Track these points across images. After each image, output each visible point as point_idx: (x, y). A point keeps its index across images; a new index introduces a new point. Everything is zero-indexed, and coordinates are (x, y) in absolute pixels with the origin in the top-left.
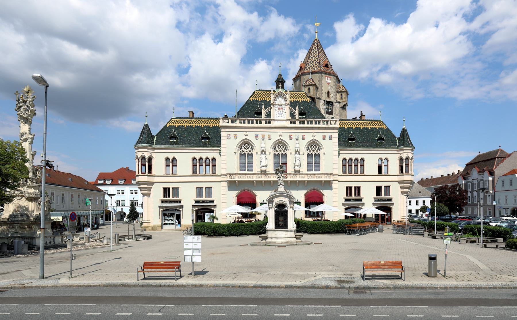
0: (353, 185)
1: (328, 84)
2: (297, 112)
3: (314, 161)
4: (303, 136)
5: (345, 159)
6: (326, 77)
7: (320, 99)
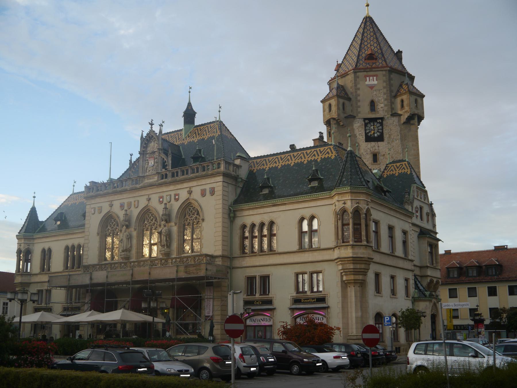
1: (372, 87)
2: (169, 161)
4: (175, 195)
5: (244, 226)
6: (366, 77)
7: (354, 117)
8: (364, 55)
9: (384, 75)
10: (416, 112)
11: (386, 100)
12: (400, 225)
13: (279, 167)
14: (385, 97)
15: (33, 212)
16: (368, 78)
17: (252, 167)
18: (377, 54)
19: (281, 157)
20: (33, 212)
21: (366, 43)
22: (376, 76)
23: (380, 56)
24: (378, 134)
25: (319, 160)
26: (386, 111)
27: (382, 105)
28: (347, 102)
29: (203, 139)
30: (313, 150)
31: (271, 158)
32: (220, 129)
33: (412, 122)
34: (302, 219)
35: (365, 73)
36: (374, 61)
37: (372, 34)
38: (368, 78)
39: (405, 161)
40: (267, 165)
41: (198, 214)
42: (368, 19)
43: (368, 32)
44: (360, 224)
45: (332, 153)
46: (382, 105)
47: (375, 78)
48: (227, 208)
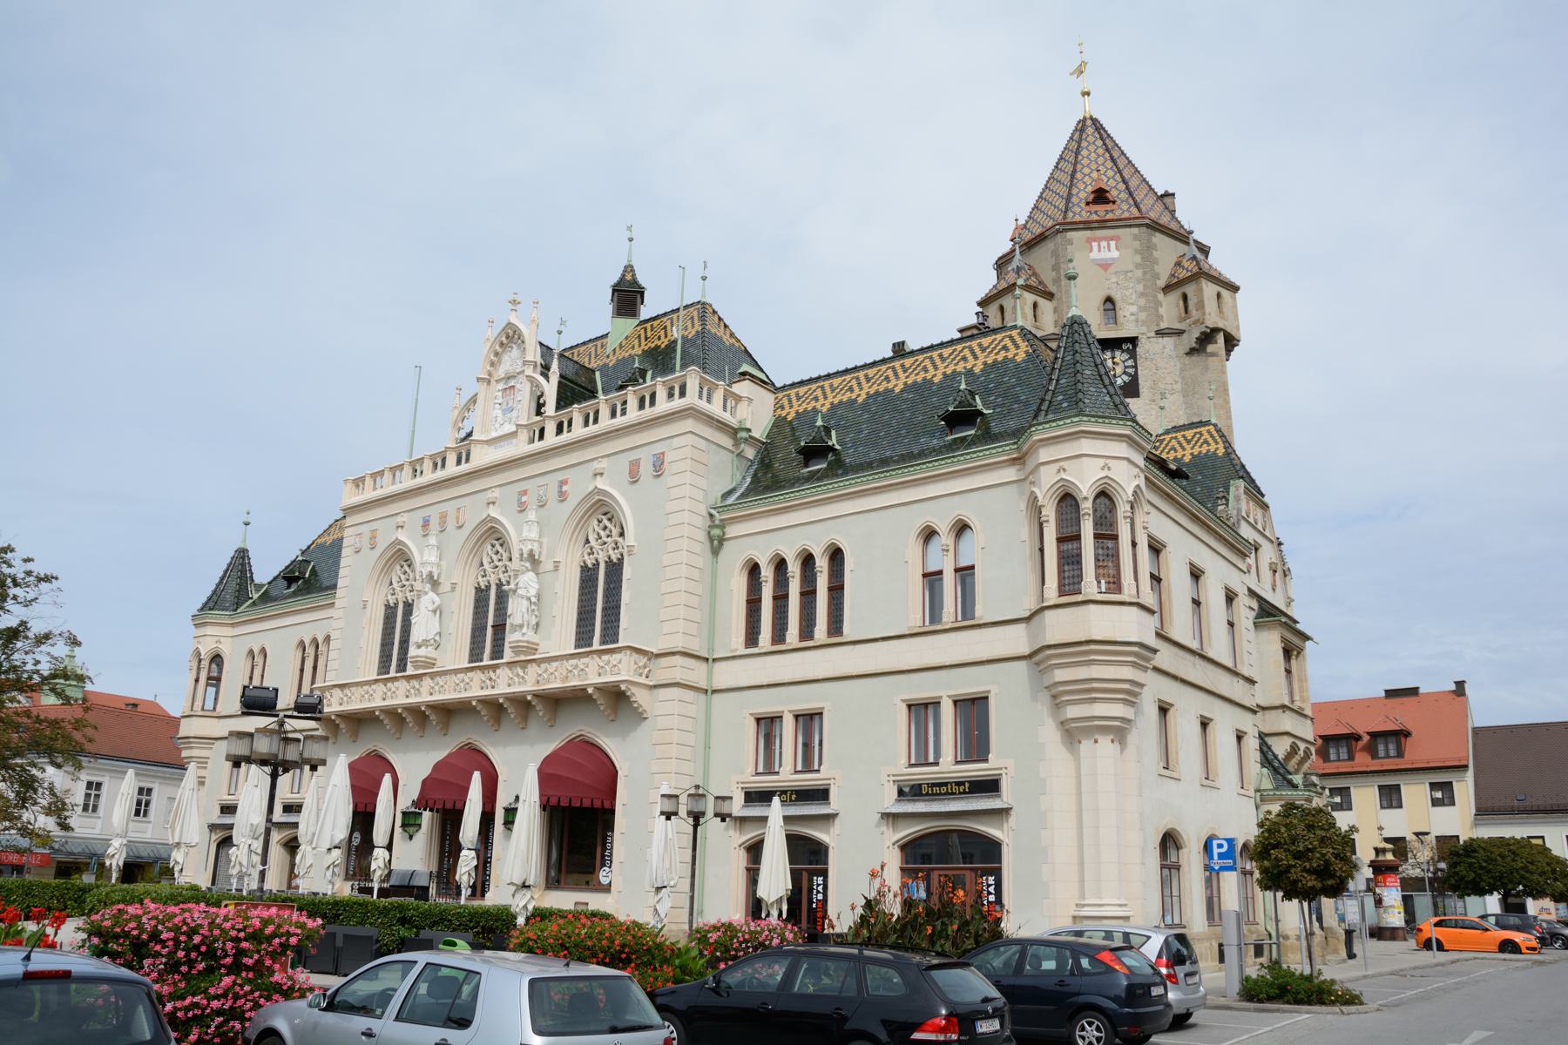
0: (787, 704)
1: (1105, 266)
3: (600, 599)
6: (1089, 241)
8: (1083, 195)
9: (1135, 237)
10: (1220, 325)
11: (1142, 295)
12: (1220, 573)
13: (860, 400)
14: (1140, 288)
15: (241, 560)
16: (1095, 244)
17: (782, 408)
18: (1114, 193)
19: (866, 376)
20: (241, 560)
21: (1087, 171)
22: (1116, 239)
23: (1124, 195)
24: (1126, 378)
25: (977, 370)
26: (1144, 323)
27: (1134, 309)
28: (1042, 302)
29: (657, 347)
30: (959, 347)
31: (836, 381)
32: (703, 319)
33: (1210, 348)
34: (929, 534)
35: (1088, 233)
36: (1109, 207)
37: (1101, 151)
38: (1095, 244)
39: (1208, 423)
40: (826, 398)
41: (622, 534)
42: (1089, 122)
43: (1092, 148)
44: (1115, 538)
45: (1017, 347)
46: (1134, 309)
47: (1113, 243)
48: (704, 513)
